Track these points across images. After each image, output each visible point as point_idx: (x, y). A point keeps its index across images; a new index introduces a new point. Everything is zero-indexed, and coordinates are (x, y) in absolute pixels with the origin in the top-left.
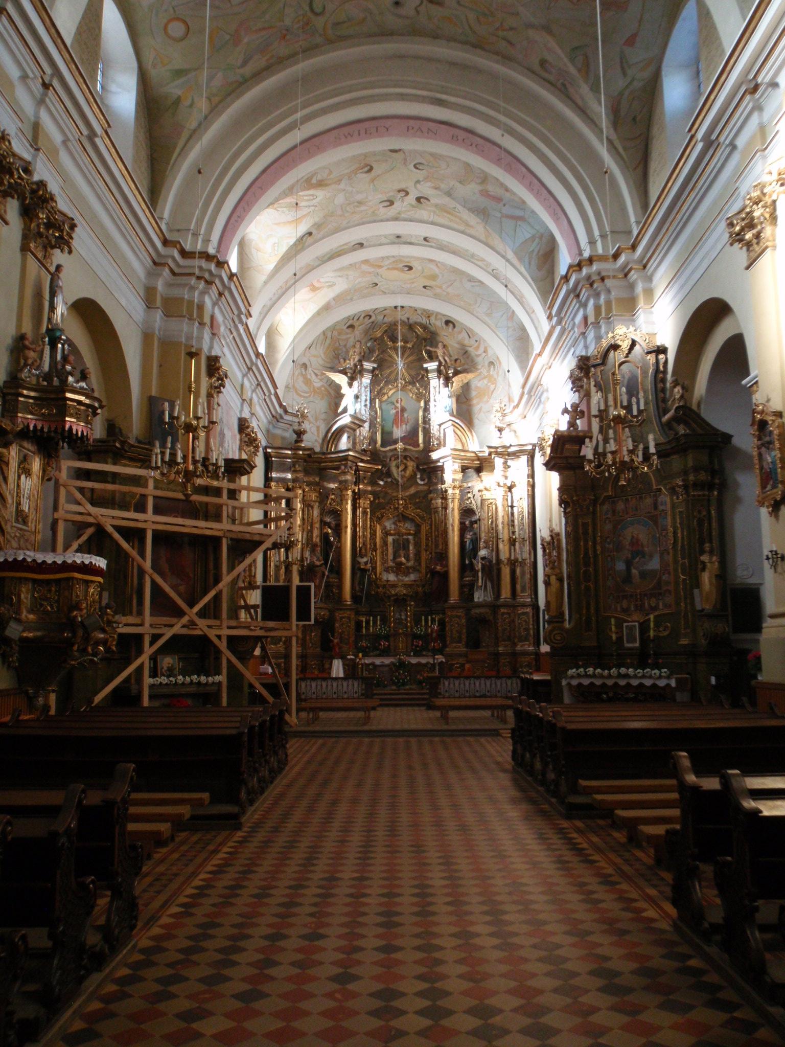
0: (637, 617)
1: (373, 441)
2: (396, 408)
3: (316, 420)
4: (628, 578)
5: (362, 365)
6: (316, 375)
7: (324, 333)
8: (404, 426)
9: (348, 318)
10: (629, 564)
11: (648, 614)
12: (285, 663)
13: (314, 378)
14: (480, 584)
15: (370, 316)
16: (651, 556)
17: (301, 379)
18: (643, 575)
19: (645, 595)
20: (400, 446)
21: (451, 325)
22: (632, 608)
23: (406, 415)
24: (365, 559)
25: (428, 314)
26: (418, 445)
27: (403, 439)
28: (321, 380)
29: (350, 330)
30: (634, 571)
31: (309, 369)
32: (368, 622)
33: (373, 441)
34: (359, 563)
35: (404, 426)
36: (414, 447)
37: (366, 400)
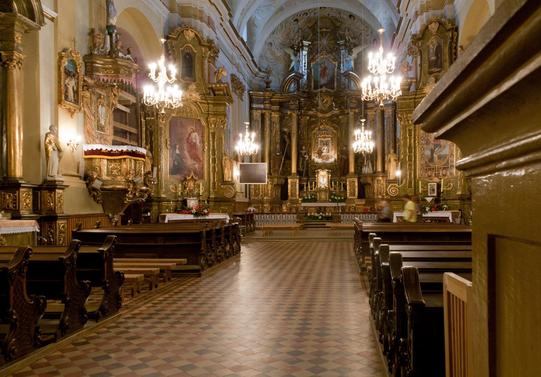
0: (436, 180)
1: (309, 86)
3: (278, 74)
4: (431, 160)
5: (302, 43)
6: (277, 49)
9: (294, 15)
10: (432, 151)
11: (441, 179)
15: (307, 14)
16: (444, 147)
17: (269, 52)
18: (440, 157)
19: (441, 168)
21: (352, 18)
22: (433, 175)
24: (304, 152)
25: (339, 11)
26: (334, 89)
27: (325, 85)
30: (435, 156)
31: (273, 46)
33: (309, 86)
34: (301, 153)
36: (332, 89)
37: (305, 63)
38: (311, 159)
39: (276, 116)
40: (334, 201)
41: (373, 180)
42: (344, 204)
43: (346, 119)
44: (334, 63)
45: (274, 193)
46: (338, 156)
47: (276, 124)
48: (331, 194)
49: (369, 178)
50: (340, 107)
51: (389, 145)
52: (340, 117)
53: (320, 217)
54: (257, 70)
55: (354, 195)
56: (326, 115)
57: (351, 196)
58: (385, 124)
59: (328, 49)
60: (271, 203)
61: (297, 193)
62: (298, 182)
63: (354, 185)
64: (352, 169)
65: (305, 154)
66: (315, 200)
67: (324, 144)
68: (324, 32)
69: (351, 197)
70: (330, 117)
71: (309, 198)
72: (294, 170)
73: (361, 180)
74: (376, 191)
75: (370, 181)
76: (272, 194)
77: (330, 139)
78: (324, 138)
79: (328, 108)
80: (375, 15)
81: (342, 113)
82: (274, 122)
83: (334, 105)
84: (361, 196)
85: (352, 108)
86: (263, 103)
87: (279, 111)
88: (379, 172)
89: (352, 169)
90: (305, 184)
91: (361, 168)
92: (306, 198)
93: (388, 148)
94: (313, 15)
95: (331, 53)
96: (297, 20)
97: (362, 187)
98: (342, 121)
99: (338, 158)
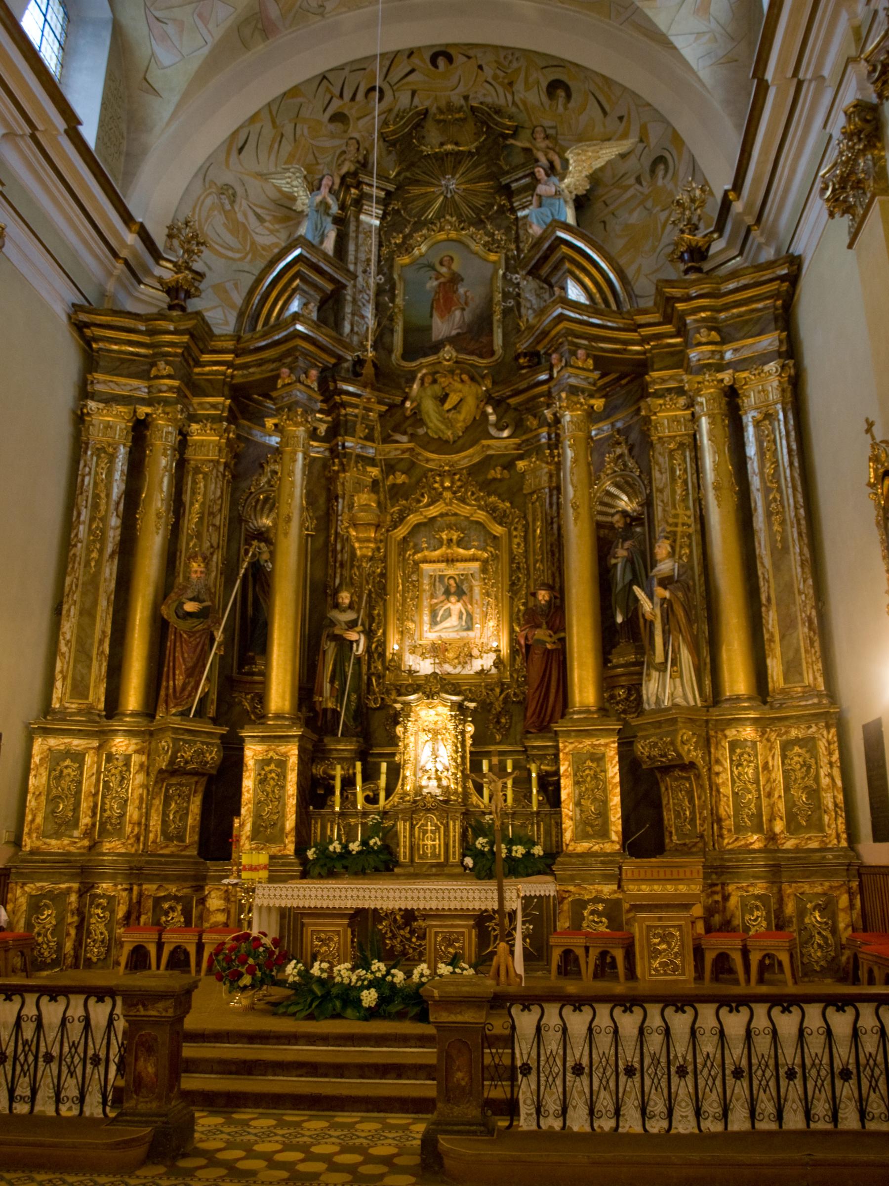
2: (439, 275)
7: (272, 110)
8: (458, 313)
12: (81, 894)
13: (253, 221)
14: (659, 657)
17: (219, 220)
20: (448, 352)
21: (561, 93)
23: (461, 291)
24: (350, 616)
25: (509, 60)
26: (492, 353)
27: (452, 340)
28: (272, 232)
29: (337, 127)
31: (242, 205)
32: (348, 782)
34: (332, 623)
35: (458, 313)
36: (481, 356)
38: (382, 655)
39: (207, 440)
40: (486, 868)
41: (707, 743)
42: (542, 887)
43: (546, 468)
44: (493, 257)
45: (155, 821)
46: (513, 640)
47: (206, 475)
48: (473, 825)
49: (685, 733)
50: (519, 427)
51: (780, 552)
52: (521, 465)
53: (369, 997)
54: (131, 238)
55: (604, 834)
56: (455, 457)
57: (586, 836)
58: (751, 450)
59: (465, 210)
60: (136, 871)
61: (290, 823)
62: (293, 760)
63: (598, 777)
64: (584, 690)
65: (352, 625)
66: (382, 861)
67: (447, 593)
68: (448, 154)
69: (583, 846)
70: (475, 470)
71: (355, 847)
72: (280, 694)
73: (641, 748)
74: (726, 808)
75: (692, 753)
76: (144, 825)
77: (475, 566)
78: (450, 561)
79: (467, 429)
80: (661, 21)
81: (529, 449)
82: (197, 470)
83: (493, 418)
84: (645, 835)
85: (574, 390)
86: (144, 375)
87: (232, 419)
88: (738, 698)
89: (584, 690)
90: (338, 772)
91: (635, 689)
92: (335, 847)
93: (776, 566)
94: (404, 99)
95: (479, 223)
96: (339, 118)
97: (644, 785)
98: (530, 483)
99: (514, 652)
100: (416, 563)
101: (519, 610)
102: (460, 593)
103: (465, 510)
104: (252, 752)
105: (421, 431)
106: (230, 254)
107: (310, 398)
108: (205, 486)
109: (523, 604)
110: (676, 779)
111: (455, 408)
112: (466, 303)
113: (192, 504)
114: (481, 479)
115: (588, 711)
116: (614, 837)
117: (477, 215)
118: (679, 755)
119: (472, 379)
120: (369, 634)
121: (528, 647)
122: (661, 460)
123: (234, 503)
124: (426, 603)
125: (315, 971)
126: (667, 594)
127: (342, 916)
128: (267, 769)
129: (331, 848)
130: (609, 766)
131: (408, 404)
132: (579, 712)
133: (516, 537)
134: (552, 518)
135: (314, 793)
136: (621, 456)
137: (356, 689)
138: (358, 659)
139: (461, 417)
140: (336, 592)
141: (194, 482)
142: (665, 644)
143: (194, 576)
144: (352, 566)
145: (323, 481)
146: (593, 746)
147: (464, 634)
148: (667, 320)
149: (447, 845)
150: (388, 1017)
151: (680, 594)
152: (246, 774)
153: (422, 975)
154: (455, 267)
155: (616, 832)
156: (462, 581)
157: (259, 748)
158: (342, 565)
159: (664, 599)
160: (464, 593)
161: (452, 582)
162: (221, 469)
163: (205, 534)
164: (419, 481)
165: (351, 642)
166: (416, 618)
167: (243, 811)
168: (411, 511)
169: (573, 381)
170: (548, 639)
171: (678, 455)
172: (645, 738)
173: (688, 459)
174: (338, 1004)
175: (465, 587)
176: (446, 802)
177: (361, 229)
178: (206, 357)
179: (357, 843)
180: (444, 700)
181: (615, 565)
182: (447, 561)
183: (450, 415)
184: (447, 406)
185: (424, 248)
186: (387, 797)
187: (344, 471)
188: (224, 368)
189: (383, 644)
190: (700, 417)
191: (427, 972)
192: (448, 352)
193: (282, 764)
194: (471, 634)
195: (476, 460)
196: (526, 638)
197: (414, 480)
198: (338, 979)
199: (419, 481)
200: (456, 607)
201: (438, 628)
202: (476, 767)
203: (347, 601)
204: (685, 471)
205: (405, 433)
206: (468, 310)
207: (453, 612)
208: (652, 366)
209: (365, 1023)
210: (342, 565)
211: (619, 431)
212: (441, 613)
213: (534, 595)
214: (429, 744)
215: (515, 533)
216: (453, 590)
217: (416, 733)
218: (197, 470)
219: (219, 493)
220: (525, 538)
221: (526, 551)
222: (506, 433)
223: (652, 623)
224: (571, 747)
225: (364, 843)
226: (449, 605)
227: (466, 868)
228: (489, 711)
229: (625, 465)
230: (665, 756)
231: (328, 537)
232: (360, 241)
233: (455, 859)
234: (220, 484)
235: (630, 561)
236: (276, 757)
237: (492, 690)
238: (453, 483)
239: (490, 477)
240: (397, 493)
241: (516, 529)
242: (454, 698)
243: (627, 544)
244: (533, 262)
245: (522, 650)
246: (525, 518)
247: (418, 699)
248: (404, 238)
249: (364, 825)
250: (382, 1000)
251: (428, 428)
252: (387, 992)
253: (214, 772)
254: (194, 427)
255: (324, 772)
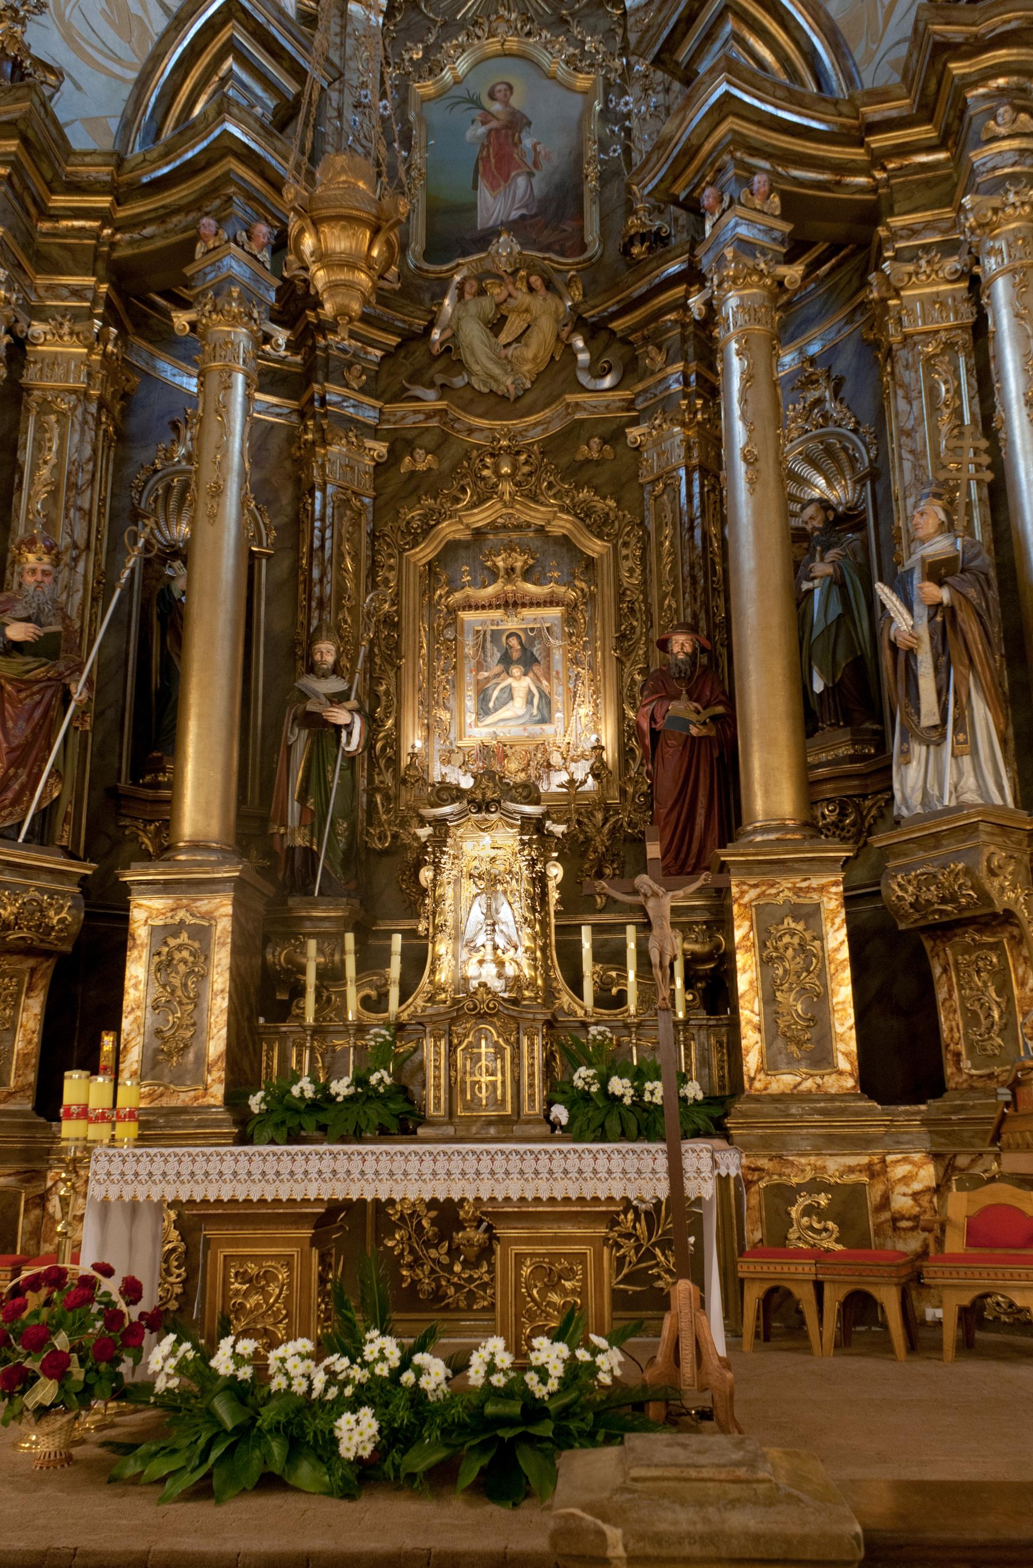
2: (487, 117)
8: (521, 181)
20: (505, 247)
23: (528, 142)
24: (335, 685)
26: (583, 247)
32: (331, 975)
34: (304, 696)
35: (521, 181)
38: (394, 762)
40: (599, 1119)
44: (582, 81)
46: (625, 731)
50: (631, 370)
52: (634, 433)
53: (357, 1433)
55: (821, 1057)
61: (216, 1045)
62: (224, 926)
65: (338, 699)
66: (396, 1114)
67: (506, 660)
69: (784, 1082)
70: (552, 447)
71: (341, 1088)
73: (900, 890)
78: (510, 604)
79: (538, 377)
82: (46, 407)
83: (584, 357)
85: (745, 246)
89: (771, 788)
92: (304, 1088)
95: (561, 23)
99: (625, 753)
100: (452, 611)
101: (633, 682)
102: (528, 661)
103: (536, 515)
104: (146, 912)
105: (459, 382)
106: (117, 69)
107: (256, 278)
108: (62, 438)
109: (641, 672)
110: (967, 950)
111: (518, 340)
112: (536, 164)
113: (35, 467)
114: (564, 461)
115: (782, 828)
116: (843, 1064)
117: (555, 10)
118: (985, 897)
119: (549, 285)
120: (372, 723)
121: (655, 734)
122: (907, 377)
123: (120, 483)
124: (469, 678)
125: (222, 1362)
126: (944, 595)
127: (297, 1220)
128: (173, 942)
129: (295, 1091)
130: (828, 928)
131: (436, 335)
132: (765, 830)
133: (626, 557)
134: (692, 521)
135: (265, 997)
136: (819, 402)
137: (348, 812)
138: (351, 760)
139: (529, 354)
140: (312, 640)
141: (40, 428)
142: (941, 692)
143: (29, 579)
144: (340, 607)
145: (288, 465)
146: (798, 891)
147: (537, 728)
148: (925, 112)
149: (517, 1083)
150: (405, 1483)
151: (972, 593)
152: (132, 955)
153: (492, 1368)
154: (515, 101)
155: (846, 1055)
156: (532, 641)
157: (158, 903)
158: (321, 605)
159: (936, 607)
160: (536, 661)
161: (514, 641)
162: (93, 408)
163: (61, 522)
164: (458, 464)
165: (338, 728)
166: (452, 703)
167: (126, 1024)
168: (442, 516)
169: (743, 231)
170: (694, 717)
171: (942, 365)
172: (906, 869)
173: (963, 371)
174: (277, 1448)
175: (537, 650)
176: (515, 1002)
177: (349, 29)
178: (60, 201)
179: (347, 1080)
180: (508, 814)
181: (810, 592)
182: (506, 605)
183: (510, 351)
184: (504, 338)
185: (462, 66)
186: (402, 1000)
187: (325, 443)
188: (95, 224)
189: (395, 741)
190: (992, 280)
191: (504, 1360)
192: (505, 247)
193: (202, 934)
194: (546, 727)
195: (555, 428)
196: (653, 719)
197: (446, 465)
198: (278, 1383)
199: (454, 469)
200: (521, 684)
201: (490, 719)
202: (568, 934)
203: (330, 659)
204: (958, 391)
205: (431, 385)
206: (538, 175)
207: (516, 694)
208: (891, 208)
209: (345, 1506)
210: (321, 605)
211: (812, 361)
212: (496, 694)
213: (663, 645)
214: (482, 899)
215: (624, 552)
216: (516, 655)
217: (457, 881)
218: (46, 407)
219: (88, 451)
220: (643, 559)
221: (645, 582)
222: (607, 382)
223: (911, 654)
224: (753, 893)
225: (360, 1081)
226: (510, 680)
227: (554, 1125)
228: (583, 855)
229: (825, 416)
230: (953, 899)
231: (298, 559)
232: (349, 51)
233: (533, 1108)
234: (90, 434)
235: (838, 582)
236: (190, 920)
237: (591, 815)
238: (515, 467)
239: (579, 457)
240: (417, 488)
241: (626, 544)
242: (528, 809)
243: (832, 554)
244: (666, 33)
245: (642, 742)
246: (641, 524)
247: (462, 814)
248: (427, 49)
249: (360, 1050)
250: (392, 1438)
251: (470, 373)
252: (403, 1416)
253: (67, 948)
254: (38, 328)
255: (288, 960)
